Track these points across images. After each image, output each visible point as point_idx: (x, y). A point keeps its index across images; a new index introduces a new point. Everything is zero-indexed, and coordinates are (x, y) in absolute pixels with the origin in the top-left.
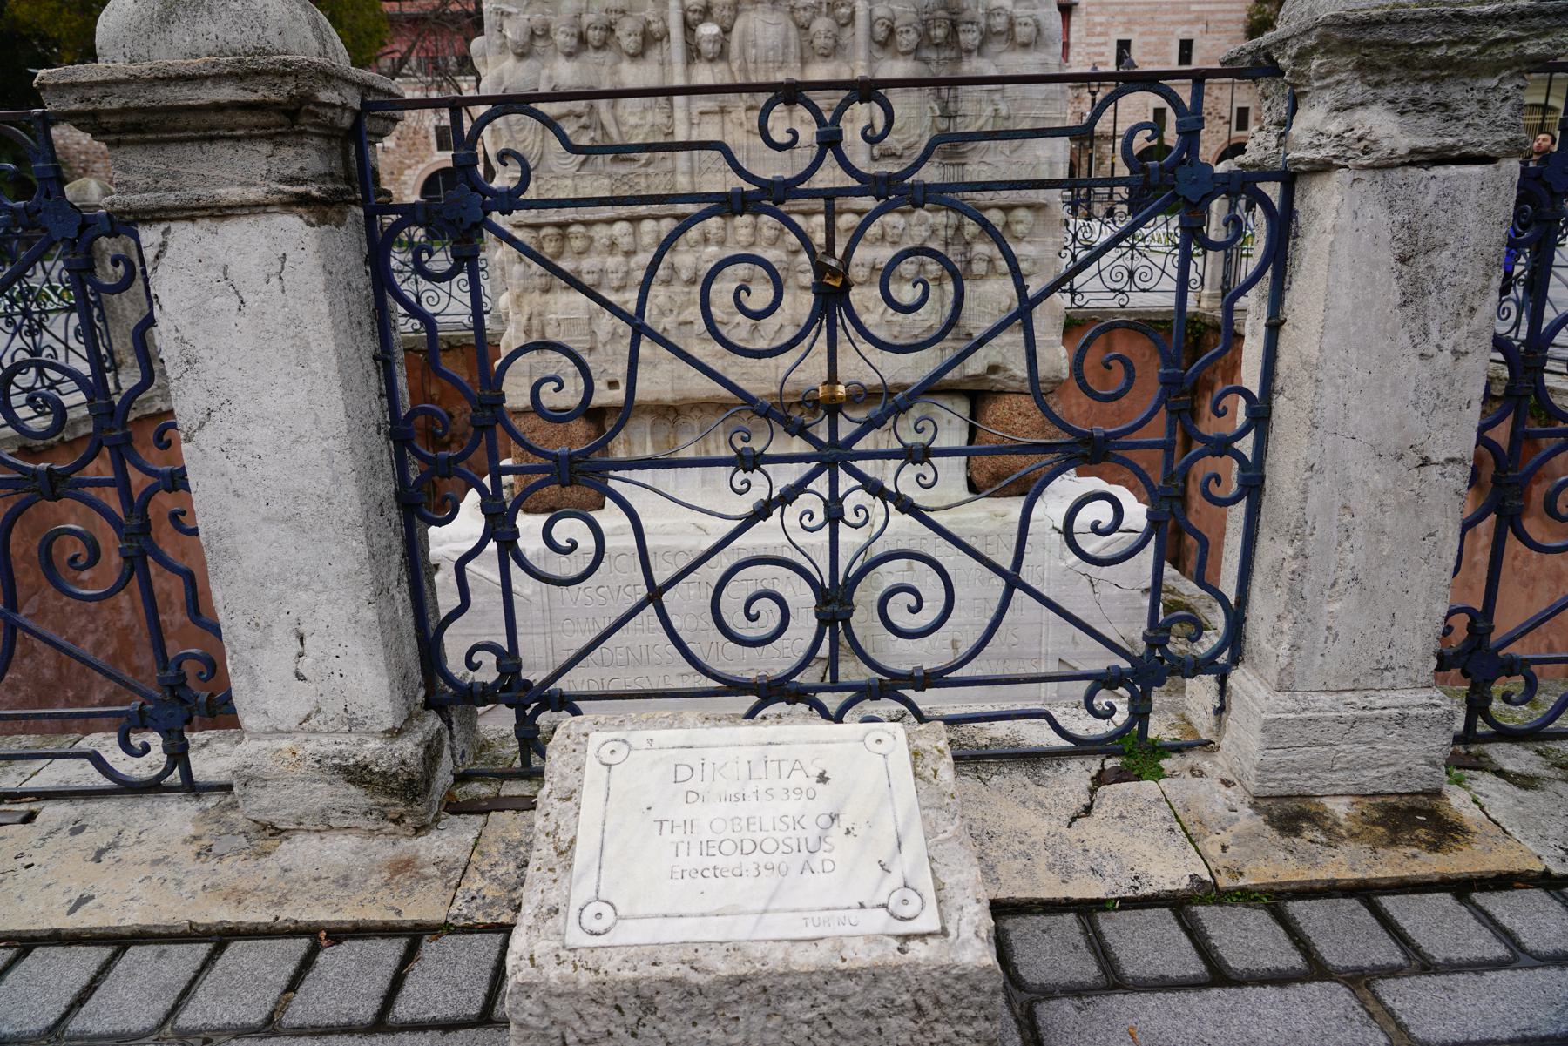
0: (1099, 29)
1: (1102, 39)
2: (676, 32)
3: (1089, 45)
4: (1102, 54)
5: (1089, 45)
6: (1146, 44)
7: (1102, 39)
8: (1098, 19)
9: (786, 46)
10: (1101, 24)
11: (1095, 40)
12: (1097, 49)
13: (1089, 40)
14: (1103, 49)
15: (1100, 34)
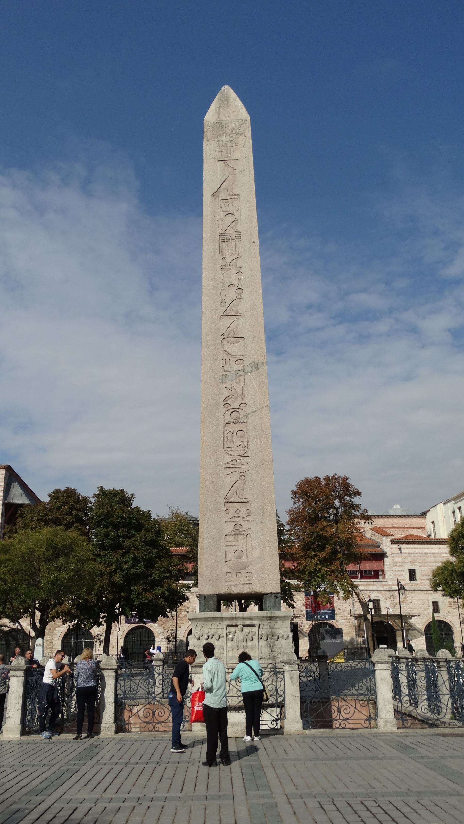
0: (398, 564)
1: (401, 569)
2: (225, 636)
3: (395, 571)
4: (402, 575)
5: (395, 571)
6: (423, 571)
7: (401, 569)
8: (397, 559)
9: (244, 639)
10: (399, 562)
11: (397, 569)
12: (399, 573)
13: (394, 569)
14: (402, 573)
15: (399, 566)
